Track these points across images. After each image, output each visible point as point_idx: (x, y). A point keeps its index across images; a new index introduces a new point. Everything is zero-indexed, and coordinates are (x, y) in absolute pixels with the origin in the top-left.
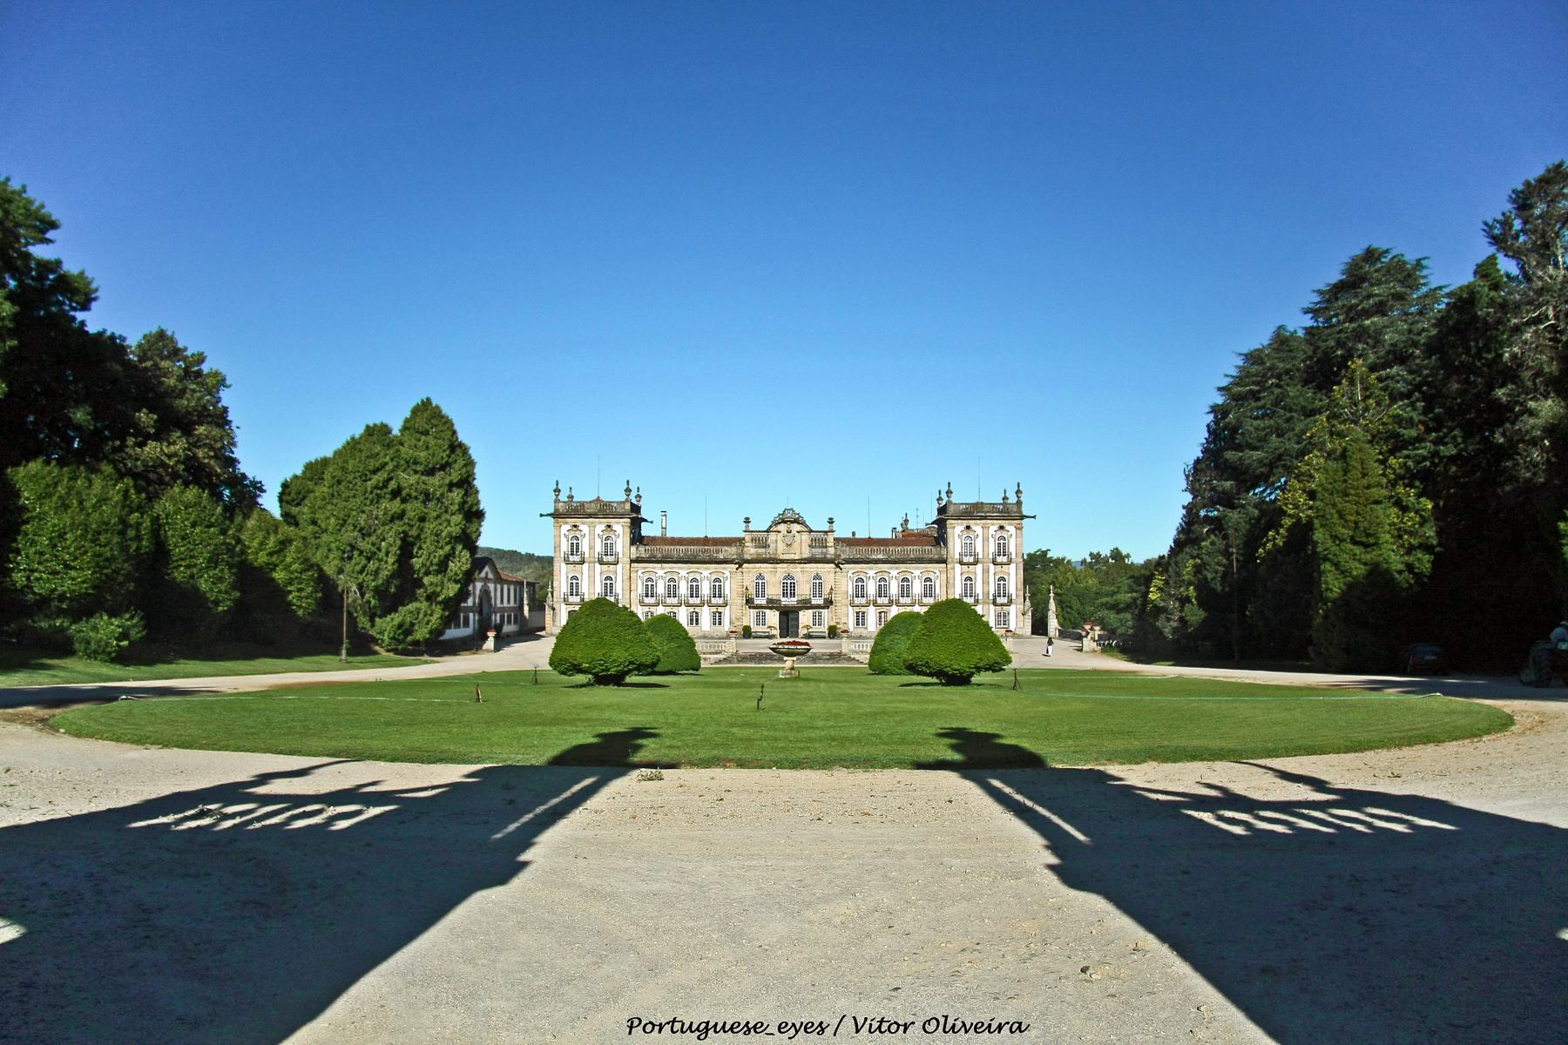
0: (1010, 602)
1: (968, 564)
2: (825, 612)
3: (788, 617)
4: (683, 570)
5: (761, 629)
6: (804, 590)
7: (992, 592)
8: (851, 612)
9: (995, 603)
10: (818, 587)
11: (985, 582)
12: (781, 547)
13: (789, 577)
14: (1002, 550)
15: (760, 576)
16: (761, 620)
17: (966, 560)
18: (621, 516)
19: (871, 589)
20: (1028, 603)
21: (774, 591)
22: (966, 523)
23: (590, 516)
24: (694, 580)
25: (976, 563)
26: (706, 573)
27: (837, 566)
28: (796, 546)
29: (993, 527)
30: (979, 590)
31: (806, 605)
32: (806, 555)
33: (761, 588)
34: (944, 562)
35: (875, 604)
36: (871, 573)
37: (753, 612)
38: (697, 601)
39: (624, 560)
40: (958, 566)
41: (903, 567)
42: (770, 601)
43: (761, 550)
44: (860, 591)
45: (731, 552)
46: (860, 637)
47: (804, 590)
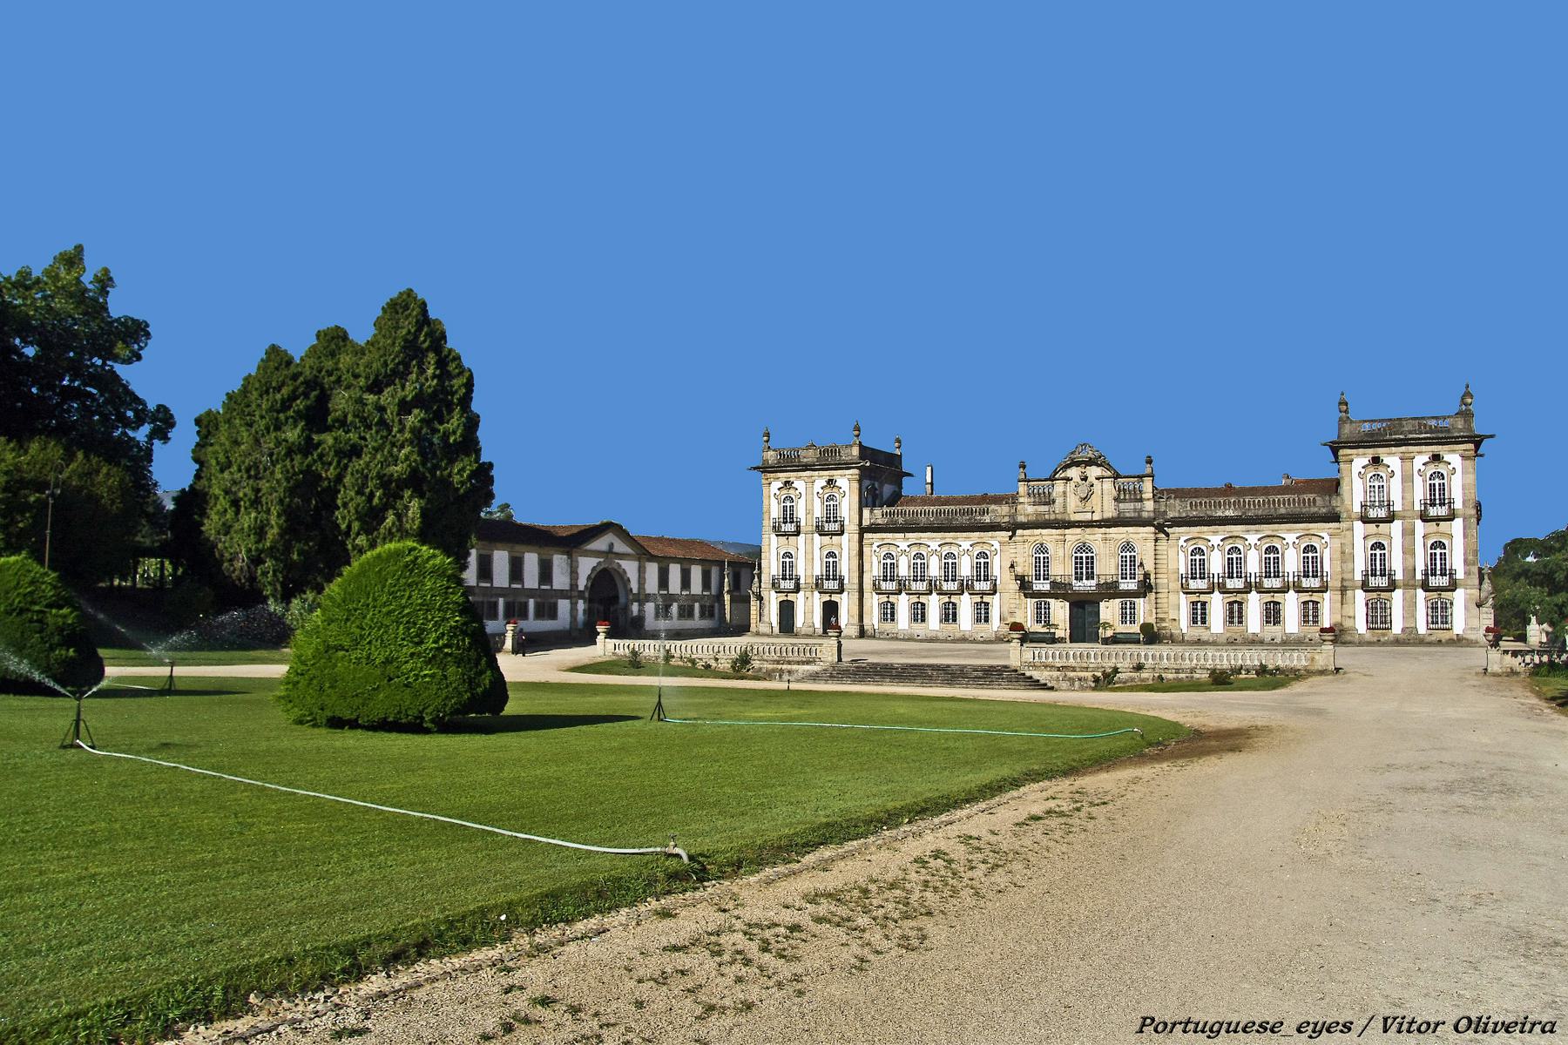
0: (1453, 586)
1: (1377, 521)
2: (1140, 602)
3: (1084, 610)
4: (933, 541)
5: (1039, 628)
6: (1107, 567)
7: (1420, 567)
8: (1184, 602)
9: (1426, 587)
10: (1130, 563)
11: (1409, 551)
12: (1073, 502)
13: (1083, 547)
14: (1438, 495)
15: (1042, 548)
16: (1042, 615)
17: (1372, 514)
18: (847, 466)
19: (1216, 564)
20: (1487, 585)
21: (1062, 568)
22: (1371, 452)
23: (806, 467)
24: (950, 555)
25: (1390, 519)
26: (966, 545)
27: (1160, 528)
28: (1095, 499)
29: (1421, 458)
30: (1397, 564)
31: (1110, 590)
32: (1110, 512)
33: (1042, 566)
34: (1334, 517)
35: (1224, 590)
36: (1216, 540)
37: (1031, 603)
38: (952, 586)
39: (851, 527)
40: (1358, 525)
41: (1267, 529)
42: (1054, 584)
43: (1045, 508)
44: (1198, 569)
45: (1001, 512)
46: (1199, 642)
47: (1107, 567)
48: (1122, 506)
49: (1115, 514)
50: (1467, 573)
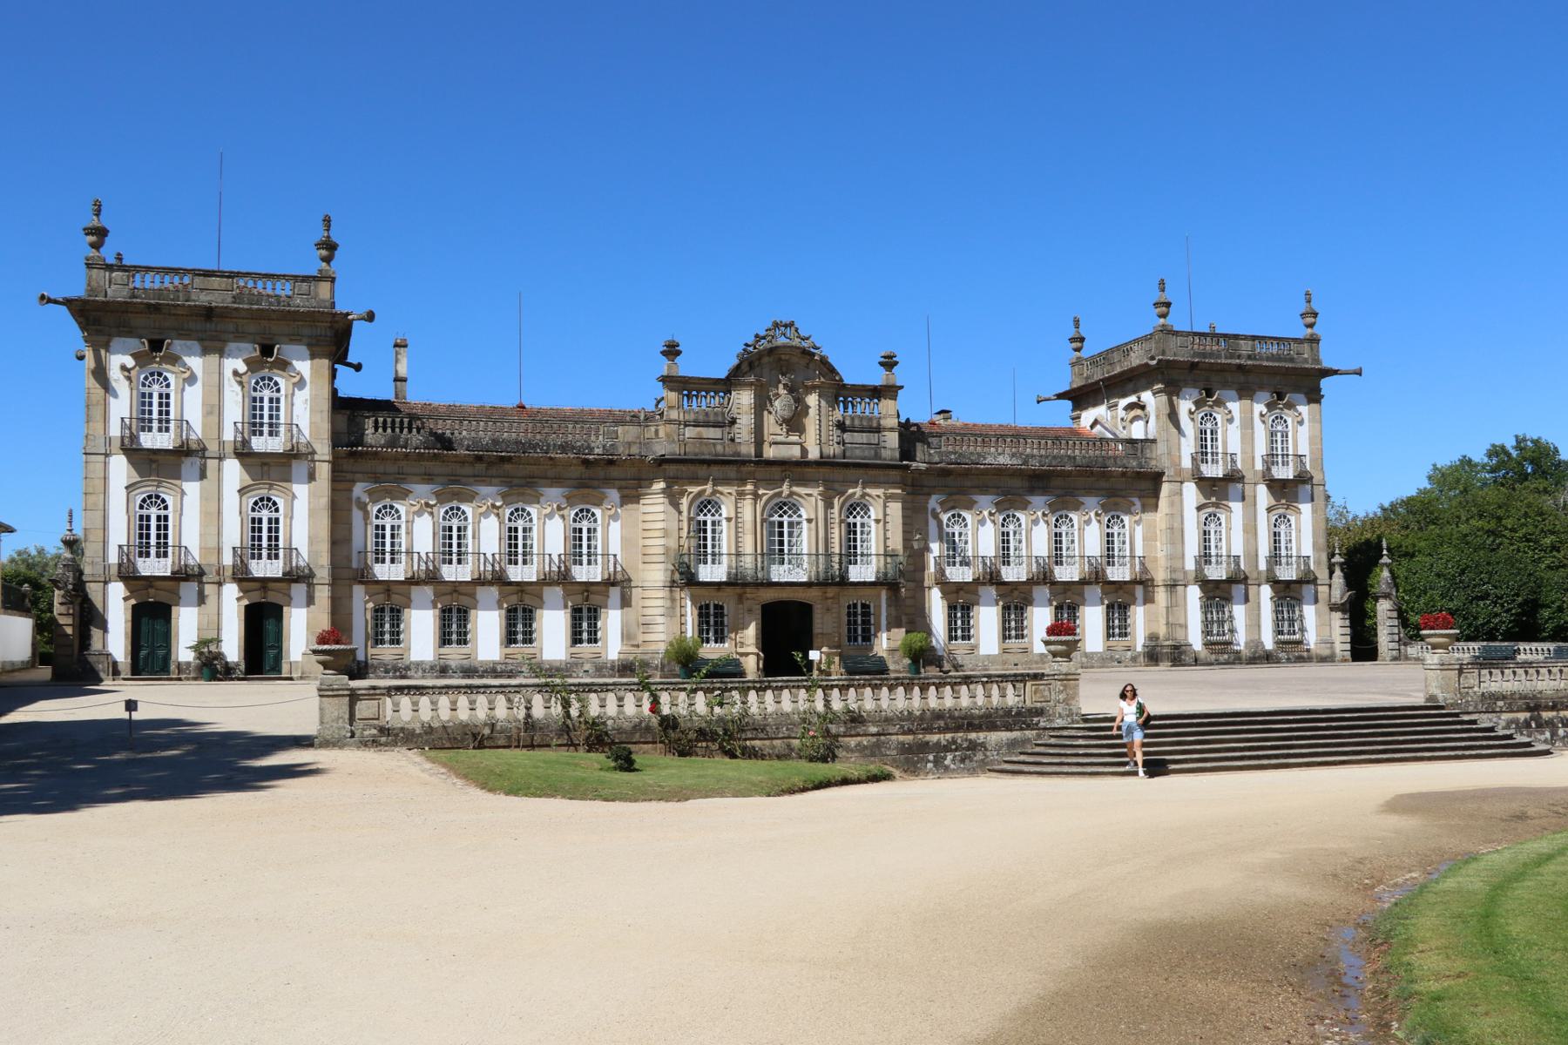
11: (1251, 529)
32: (833, 449)
48: (847, 436)
49: (838, 449)
50: (1318, 563)
